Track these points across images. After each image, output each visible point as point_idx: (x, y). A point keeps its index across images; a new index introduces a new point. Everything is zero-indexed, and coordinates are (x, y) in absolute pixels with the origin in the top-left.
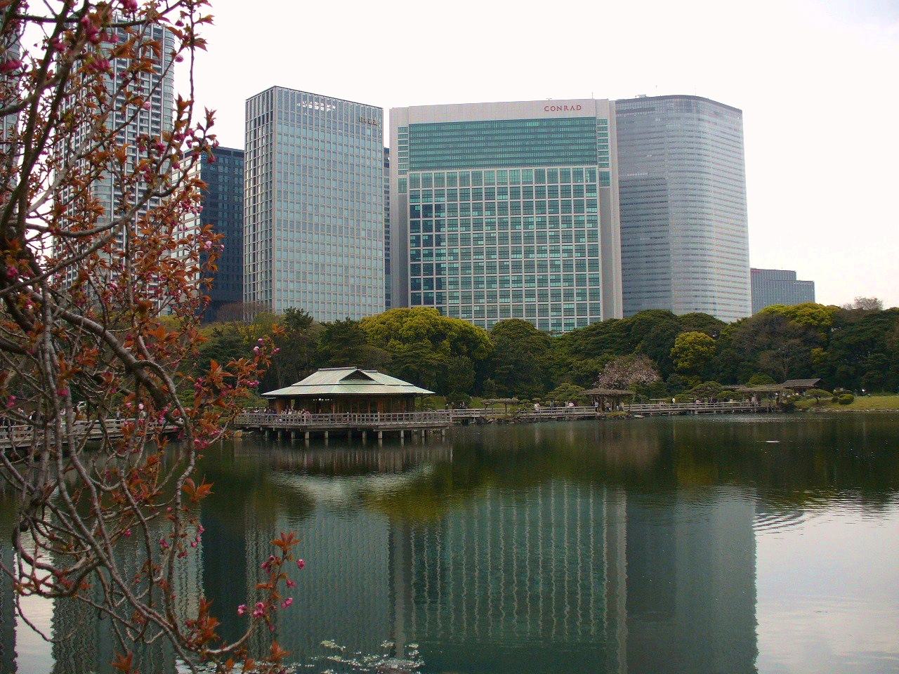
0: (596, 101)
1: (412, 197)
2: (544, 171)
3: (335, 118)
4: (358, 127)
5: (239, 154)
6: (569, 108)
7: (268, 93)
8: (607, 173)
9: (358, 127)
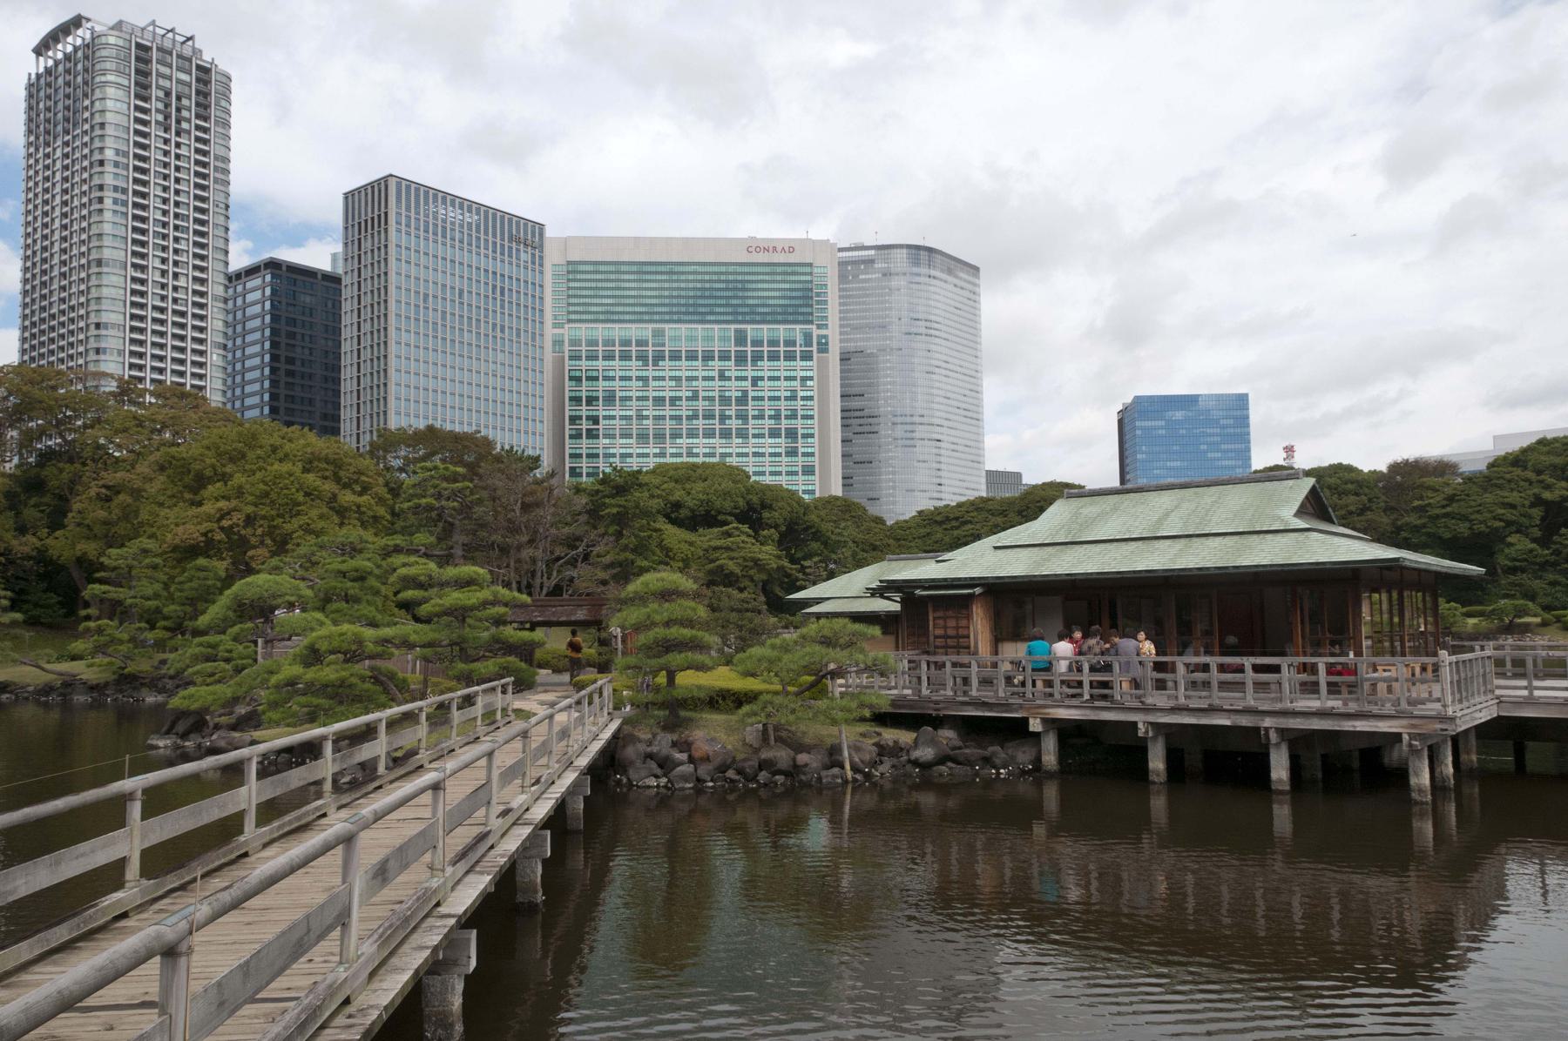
0: (814, 241)
3: (478, 231)
4: (510, 248)
5: (332, 280)
6: (779, 249)
7: (373, 187)
8: (825, 337)
9: (510, 248)
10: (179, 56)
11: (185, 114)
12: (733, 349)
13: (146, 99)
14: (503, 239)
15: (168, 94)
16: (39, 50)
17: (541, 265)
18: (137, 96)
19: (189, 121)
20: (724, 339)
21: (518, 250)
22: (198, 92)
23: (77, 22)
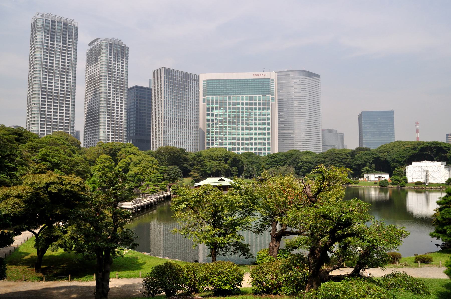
1: (207, 105)
2: (252, 97)
4: (191, 82)
5: (150, 89)
6: (261, 75)
8: (274, 98)
9: (191, 82)
10: (118, 45)
11: (119, 58)
12: (249, 102)
13: (111, 56)
14: (189, 80)
15: (116, 54)
16: (89, 45)
17: (198, 85)
18: (110, 55)
19: (120, 59)
20: (247, 99)
21: (193, 82)
22: (122, 52)
23: (97, 39)
